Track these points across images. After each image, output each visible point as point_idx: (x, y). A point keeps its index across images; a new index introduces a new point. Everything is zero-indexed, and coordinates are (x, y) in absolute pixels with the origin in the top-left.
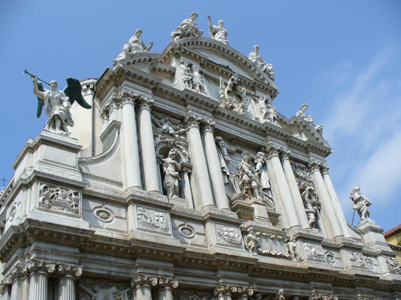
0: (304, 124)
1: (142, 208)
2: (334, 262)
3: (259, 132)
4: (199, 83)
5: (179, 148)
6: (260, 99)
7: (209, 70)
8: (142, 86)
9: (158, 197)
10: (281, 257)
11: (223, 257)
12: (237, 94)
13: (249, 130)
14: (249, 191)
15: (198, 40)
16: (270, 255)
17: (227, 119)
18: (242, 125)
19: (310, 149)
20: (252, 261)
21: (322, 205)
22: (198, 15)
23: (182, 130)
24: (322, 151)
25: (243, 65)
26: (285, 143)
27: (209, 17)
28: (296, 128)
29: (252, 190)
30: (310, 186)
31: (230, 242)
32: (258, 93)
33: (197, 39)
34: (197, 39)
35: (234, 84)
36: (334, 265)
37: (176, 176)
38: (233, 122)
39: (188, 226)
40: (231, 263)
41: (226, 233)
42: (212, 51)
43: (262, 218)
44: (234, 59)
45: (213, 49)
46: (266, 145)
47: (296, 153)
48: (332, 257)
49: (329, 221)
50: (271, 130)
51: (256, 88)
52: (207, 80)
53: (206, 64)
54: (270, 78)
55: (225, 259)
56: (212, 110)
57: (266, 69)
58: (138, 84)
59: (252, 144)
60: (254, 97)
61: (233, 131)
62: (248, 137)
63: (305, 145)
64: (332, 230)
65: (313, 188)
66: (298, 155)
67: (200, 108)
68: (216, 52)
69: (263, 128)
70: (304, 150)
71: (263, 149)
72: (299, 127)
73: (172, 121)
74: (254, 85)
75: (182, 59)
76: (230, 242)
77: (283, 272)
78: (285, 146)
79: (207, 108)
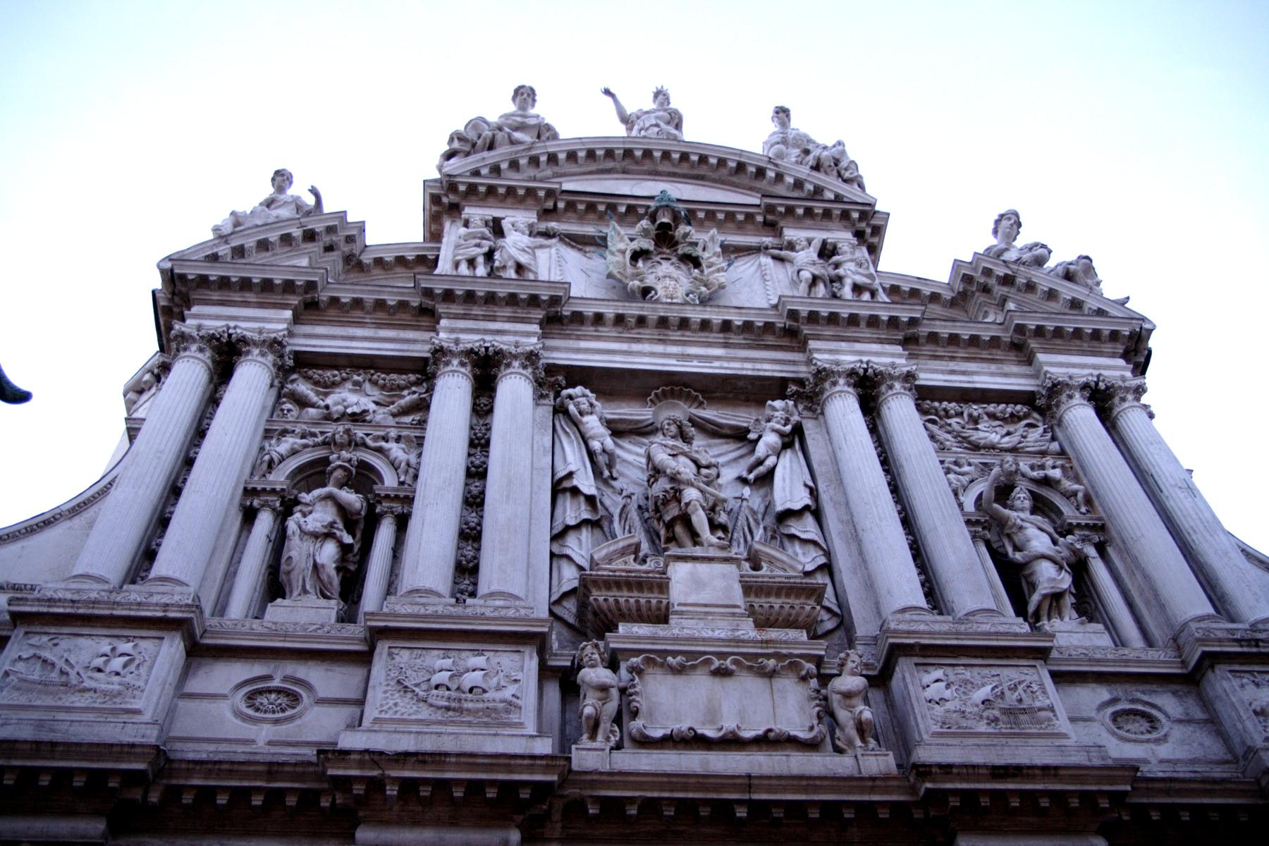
0: (1001, 271)
1: (45, 639)
2: (1165, 738)
3: (770, 340)
4: (511, 257)
5: (380, 450)
6: (798, 247)
7: (581, 218)
8: (261, 305)
9: (151, 594)
10: (767, 741)
11: (361, 764)
12: (680, 252)
13: (726, 345)
14: (679, 529)
15: (533, 152)
16: (696, 741)
17: (620, 329)
18: (688, 333)
19: (1033, 344)
20: (531, 769)
21: (1109, 524)
22: (532, 90)
23: (408, 398)
24: (1096, 335)
25: (734, 179)
26: (899, 349)
27: (607, 92)
28: (981, 298)
29: (685, 520)
30: (1042, 467)
31: (448, 709)
32: (790, 234)
33: (530, 149)
34: (530, 149)
35: (663, 226)
36: (1164, 751)
37: (325, 531)
38: (646, 333)
39: (285, 679)
40: (408, 786)
41: (443, 677)
42: (609, 171)
43: (706, 606)
44: (696, 172)
45: (610, 164)
46: (801, 376)
47: (964, 373)
48: (1151, 719)
49: (1147, 577)
50: (813, 317)
51: (782, 224)
52: (580, 250)
53: (561, 205)
54: (845, 181)
55: (375, 773)
56: (539, 314)
57: (818, 160)
58: (246, 304)
59: (740, 384)
60: (776, 252)
61: (646, 360)
62: (717, 364)
63: (1006, 337)
64: (1162, 607)
65: (1056, 473)
66: (976, 378)
67: (493, 319)
68: (624, 172)
69: (780, 322)
70: (1012, 356)
71: (793, 388)
72: (986, 290)
73: (381, 382)
74: (770, 217)
75: (470, 211)
76: (448, 709)
77: (758, 808)
78: (900, 356)
79: (521, 313)
